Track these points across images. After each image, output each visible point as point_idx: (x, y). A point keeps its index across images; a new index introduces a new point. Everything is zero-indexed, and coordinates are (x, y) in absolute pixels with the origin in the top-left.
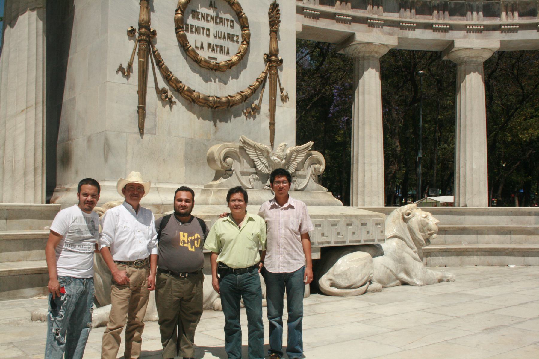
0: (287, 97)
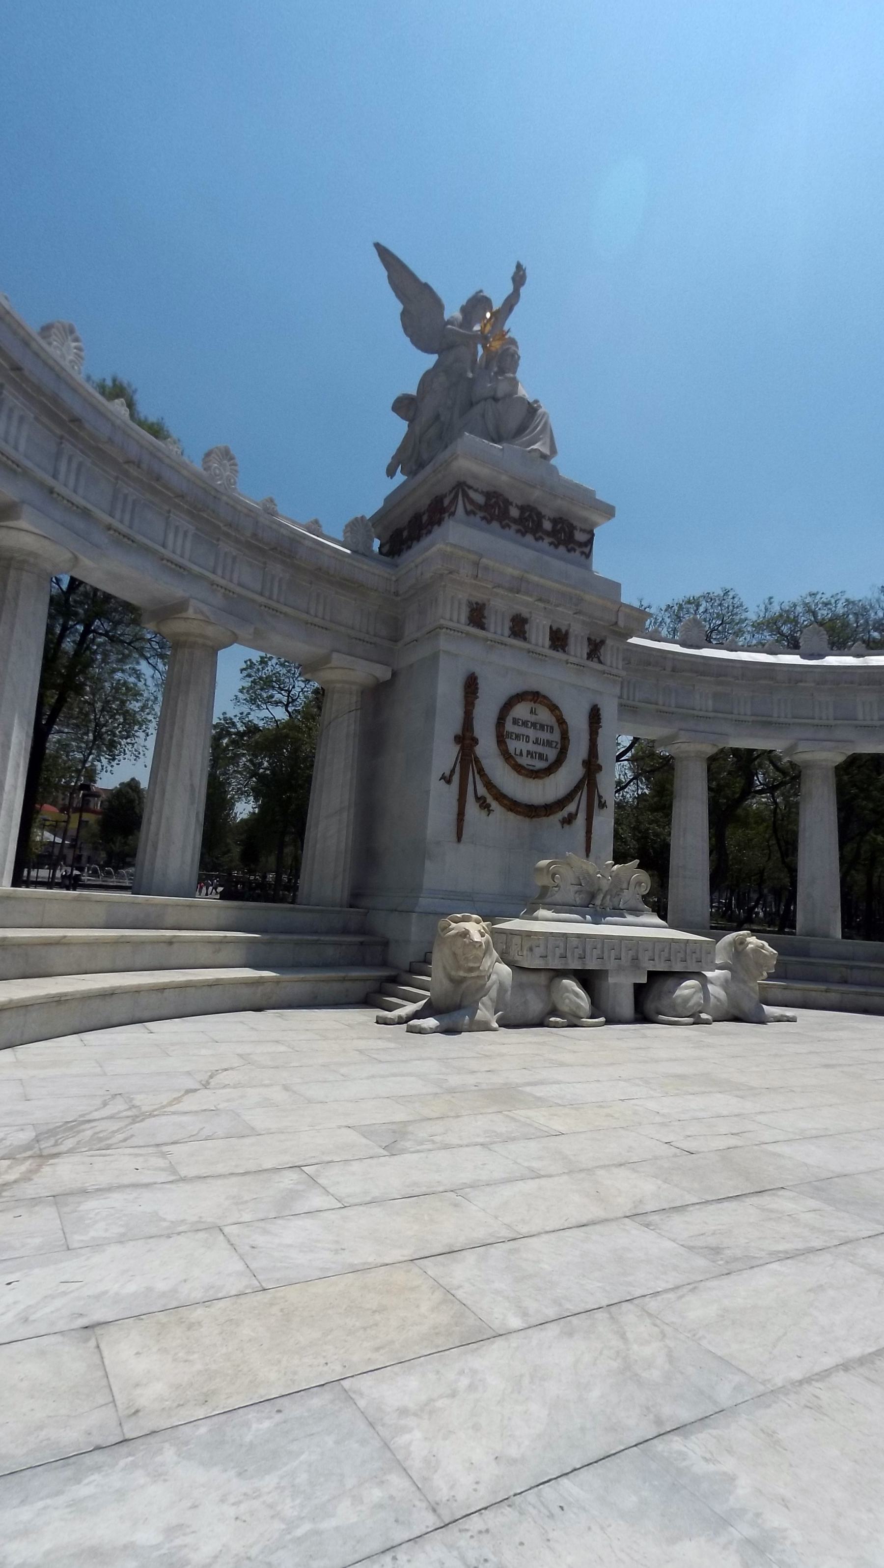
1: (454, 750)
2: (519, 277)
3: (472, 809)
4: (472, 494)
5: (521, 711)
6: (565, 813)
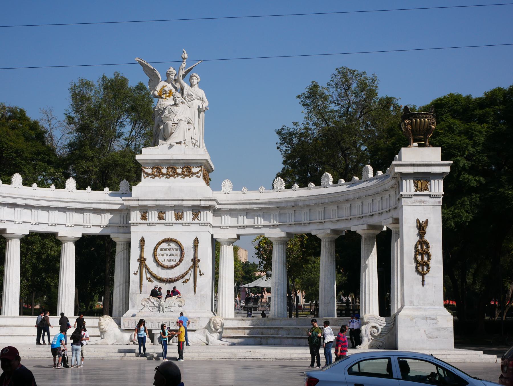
0: (203, 274)
1: (138, 264)
3: (145, 281)
4: (146, 170)
5: (164, 246)
6: (184, 280)
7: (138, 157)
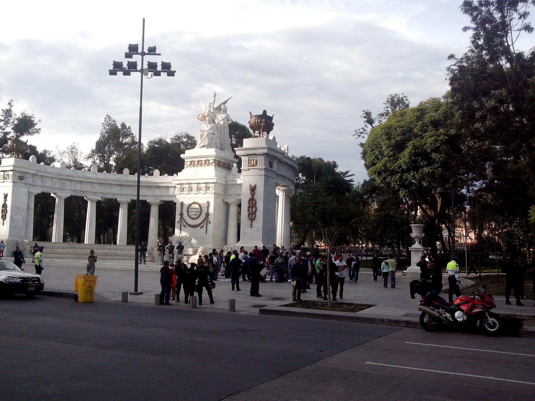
2: (215, 96)
3: (182, 227)
6: (201, 226)
7: (182, 156)
